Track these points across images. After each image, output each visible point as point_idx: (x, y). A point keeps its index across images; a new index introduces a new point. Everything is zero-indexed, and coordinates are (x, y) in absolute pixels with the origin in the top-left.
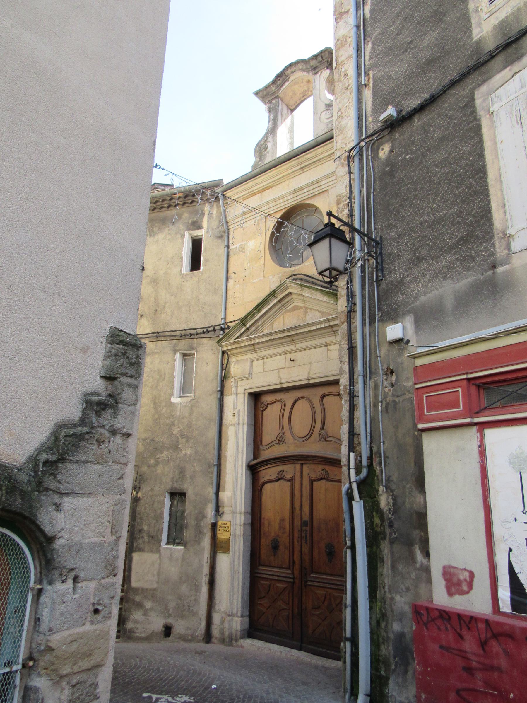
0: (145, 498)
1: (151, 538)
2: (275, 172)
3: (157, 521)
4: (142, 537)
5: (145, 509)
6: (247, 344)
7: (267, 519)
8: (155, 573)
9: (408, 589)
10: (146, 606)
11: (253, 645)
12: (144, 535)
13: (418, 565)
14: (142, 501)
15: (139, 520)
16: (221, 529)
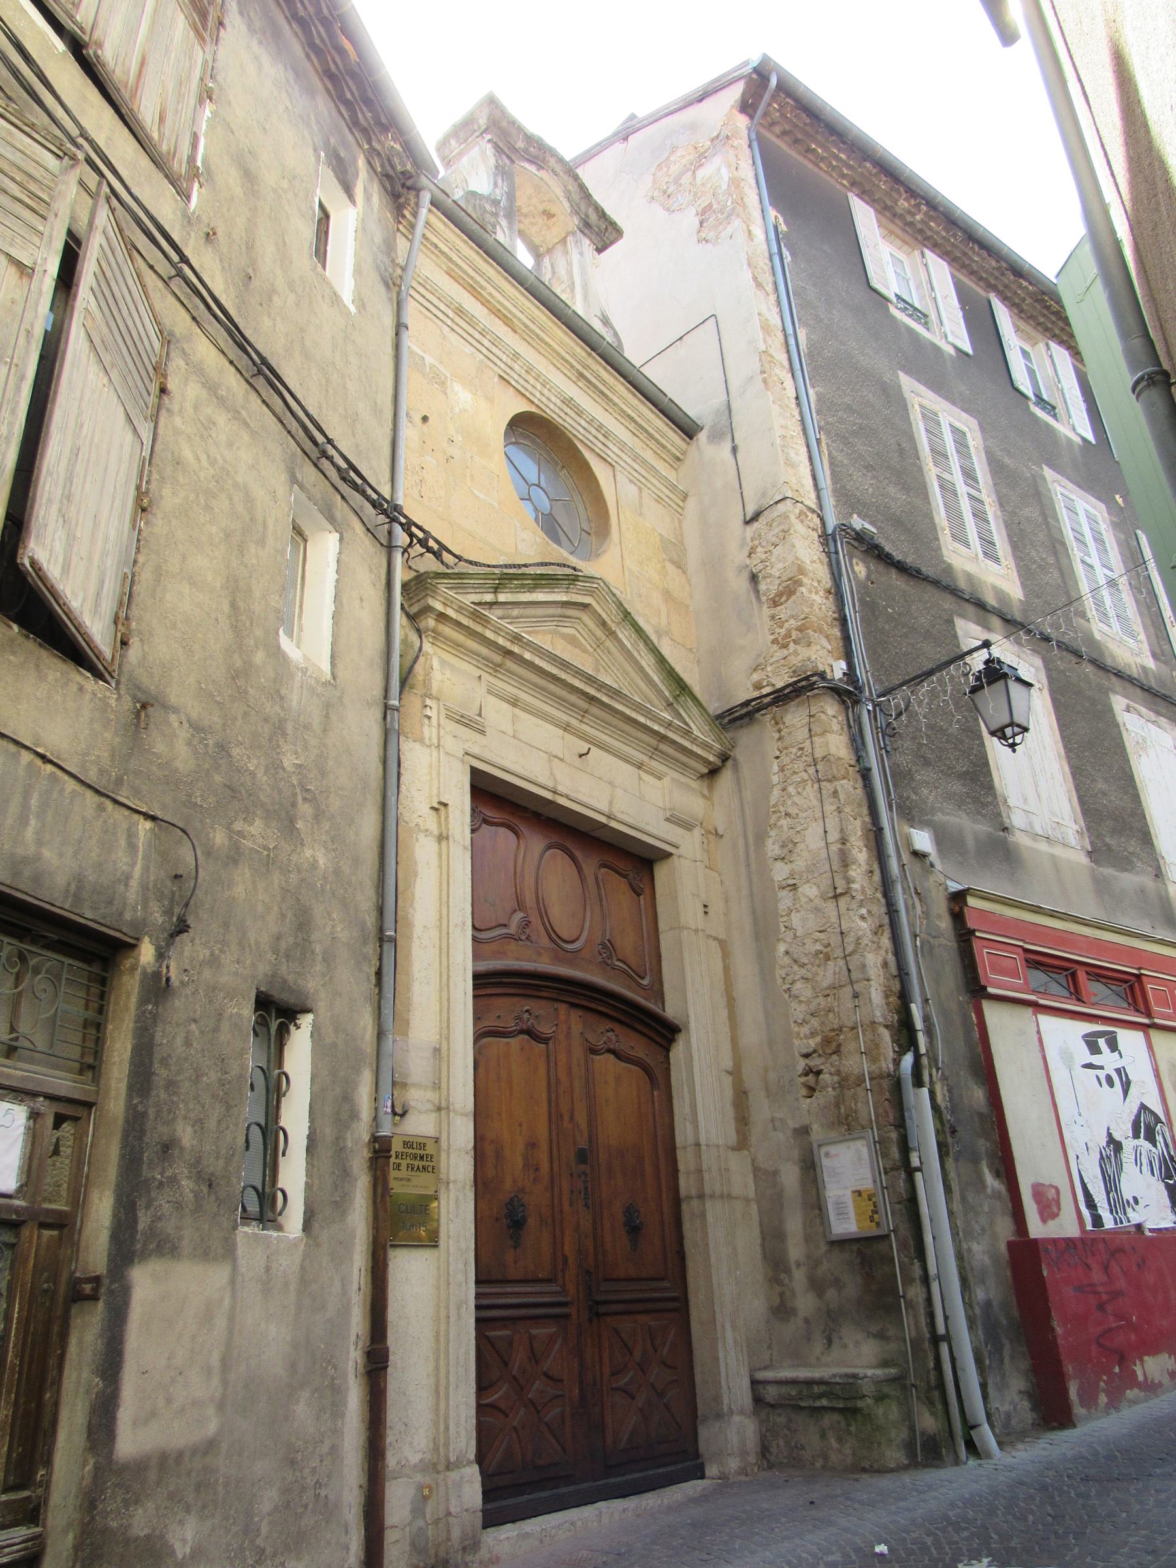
0: (188, 991)
1: (205, 1189)
2: (544, 318)
3: (229, 1107)
4: (174, 1180)
5: (188, 1043)
6: (501, 641)
7: (492, 1142)
8: (215, 1360)
9: (983, 1229)
10: (177, 1546)
11: (527, 1535)
12: (180, 1170)
13: (989, 1191)
14: (178, 1003)
15: (163, 1095)
16: (404, 1163)
